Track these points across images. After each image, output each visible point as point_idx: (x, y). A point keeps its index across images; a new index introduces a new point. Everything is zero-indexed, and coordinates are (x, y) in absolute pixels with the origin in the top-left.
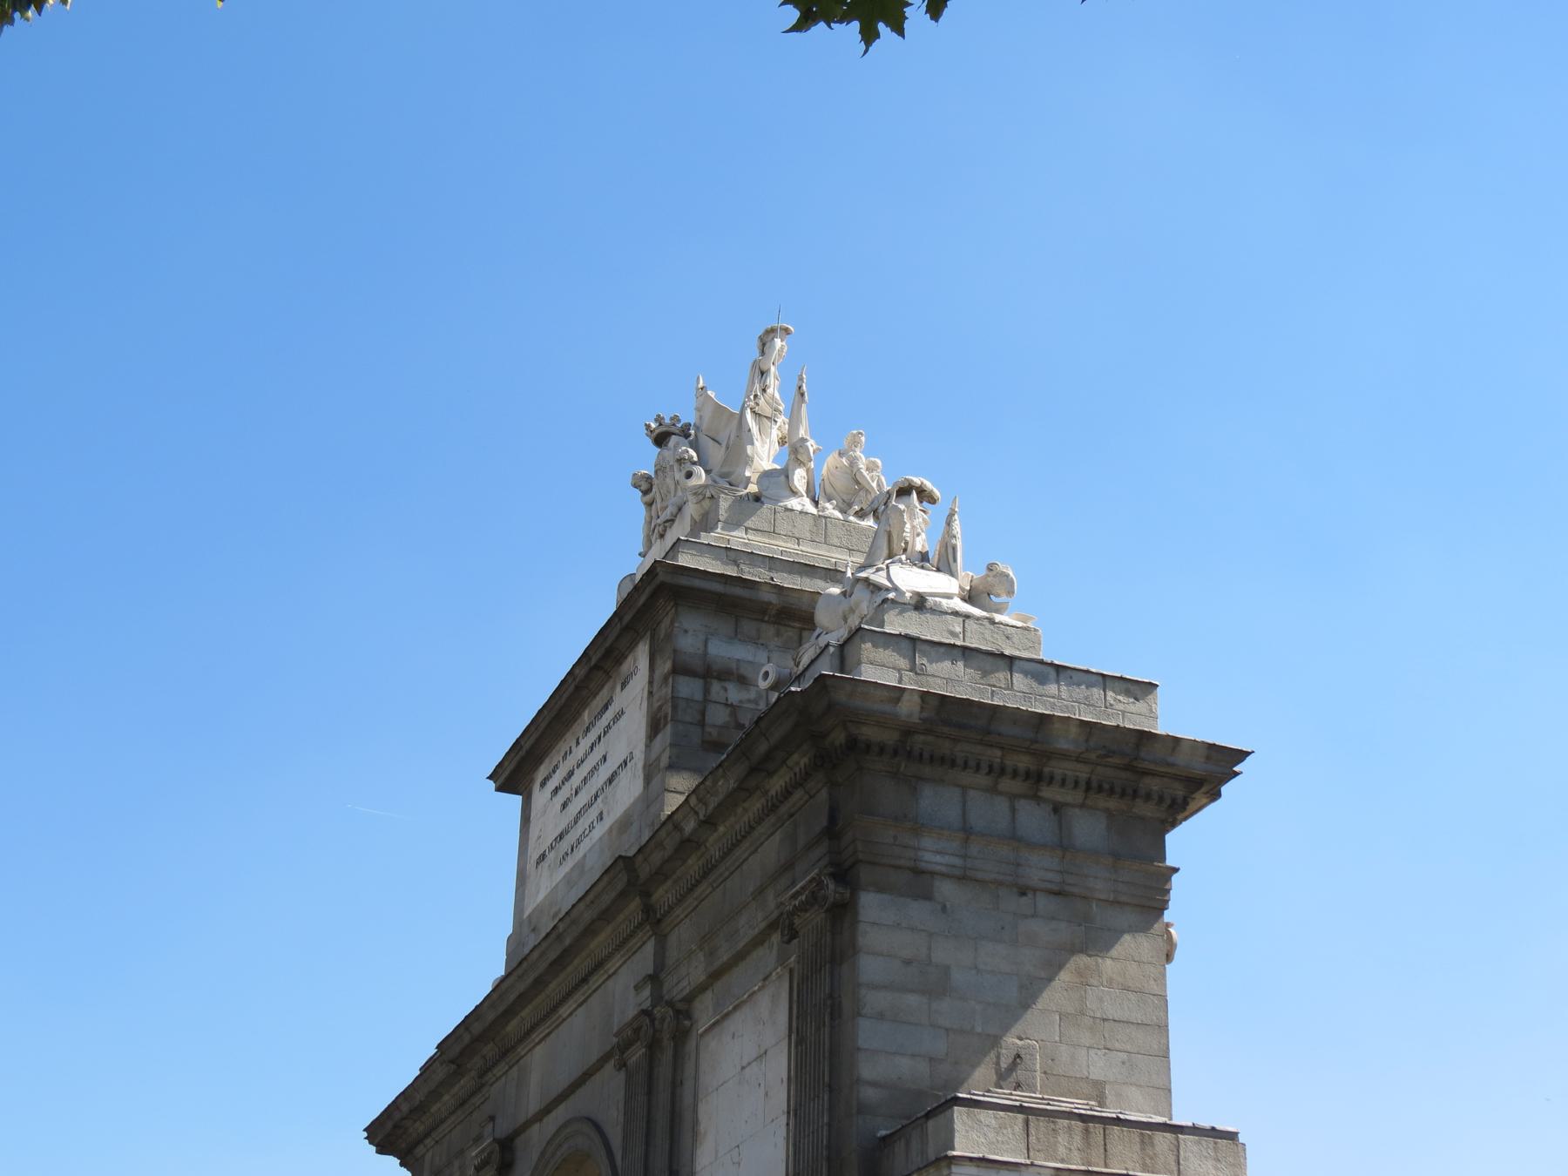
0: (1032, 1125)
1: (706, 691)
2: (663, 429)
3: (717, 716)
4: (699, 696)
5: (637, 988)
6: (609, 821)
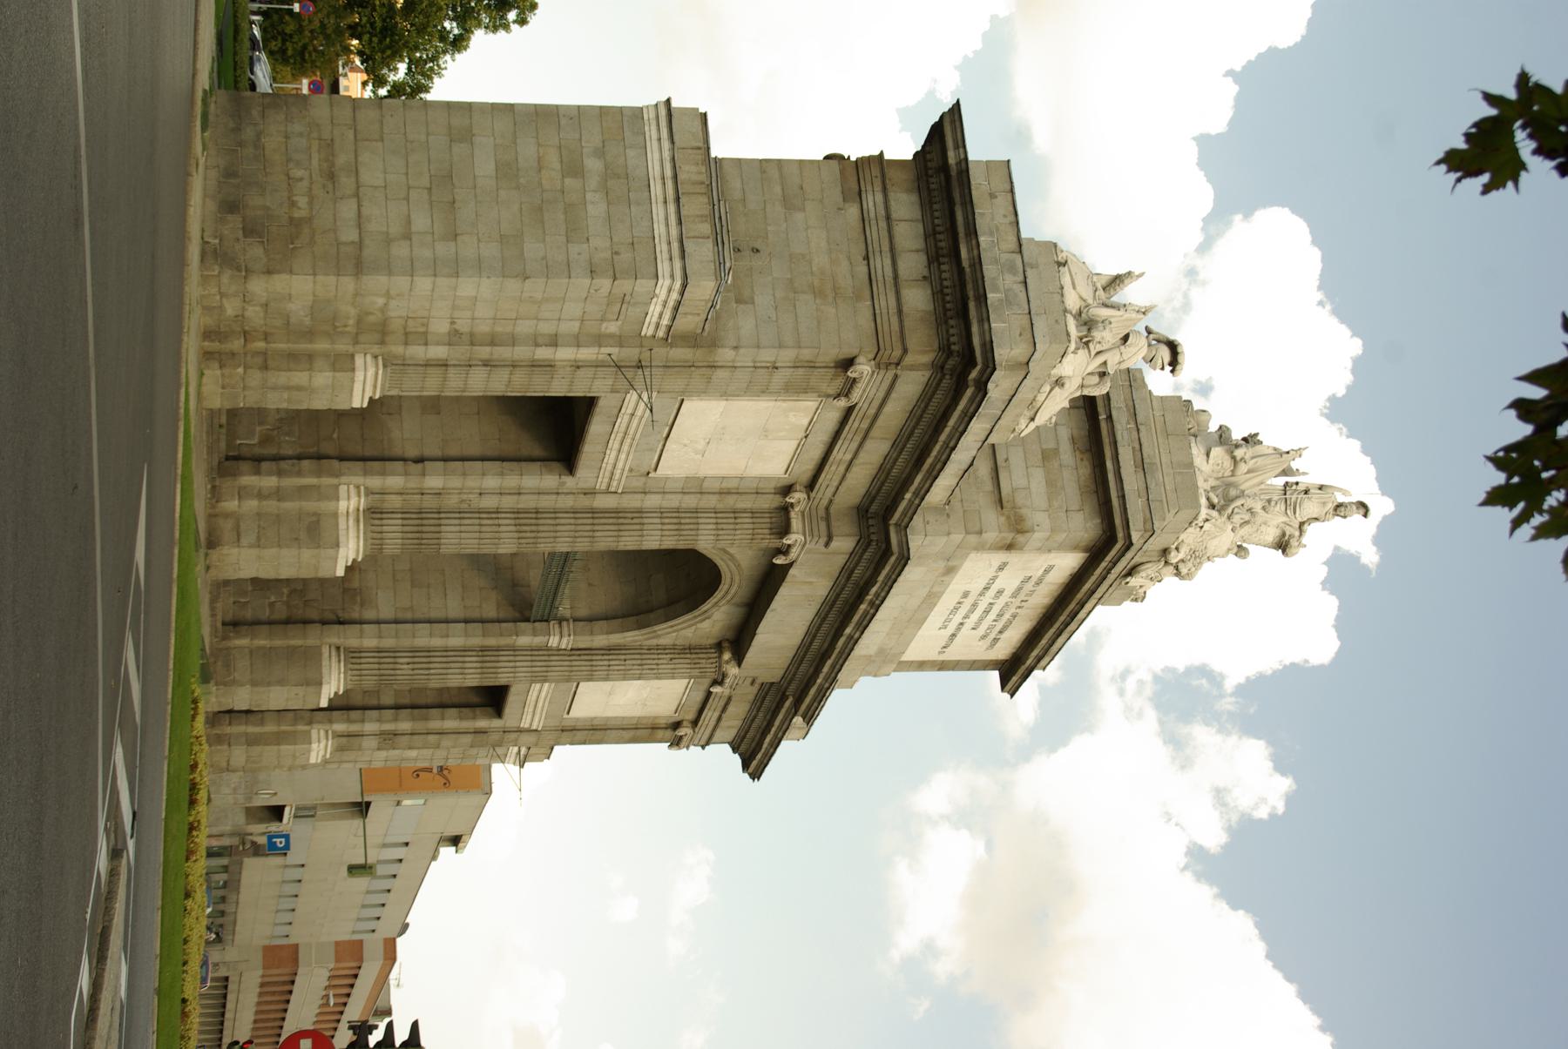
0: (699, 151)
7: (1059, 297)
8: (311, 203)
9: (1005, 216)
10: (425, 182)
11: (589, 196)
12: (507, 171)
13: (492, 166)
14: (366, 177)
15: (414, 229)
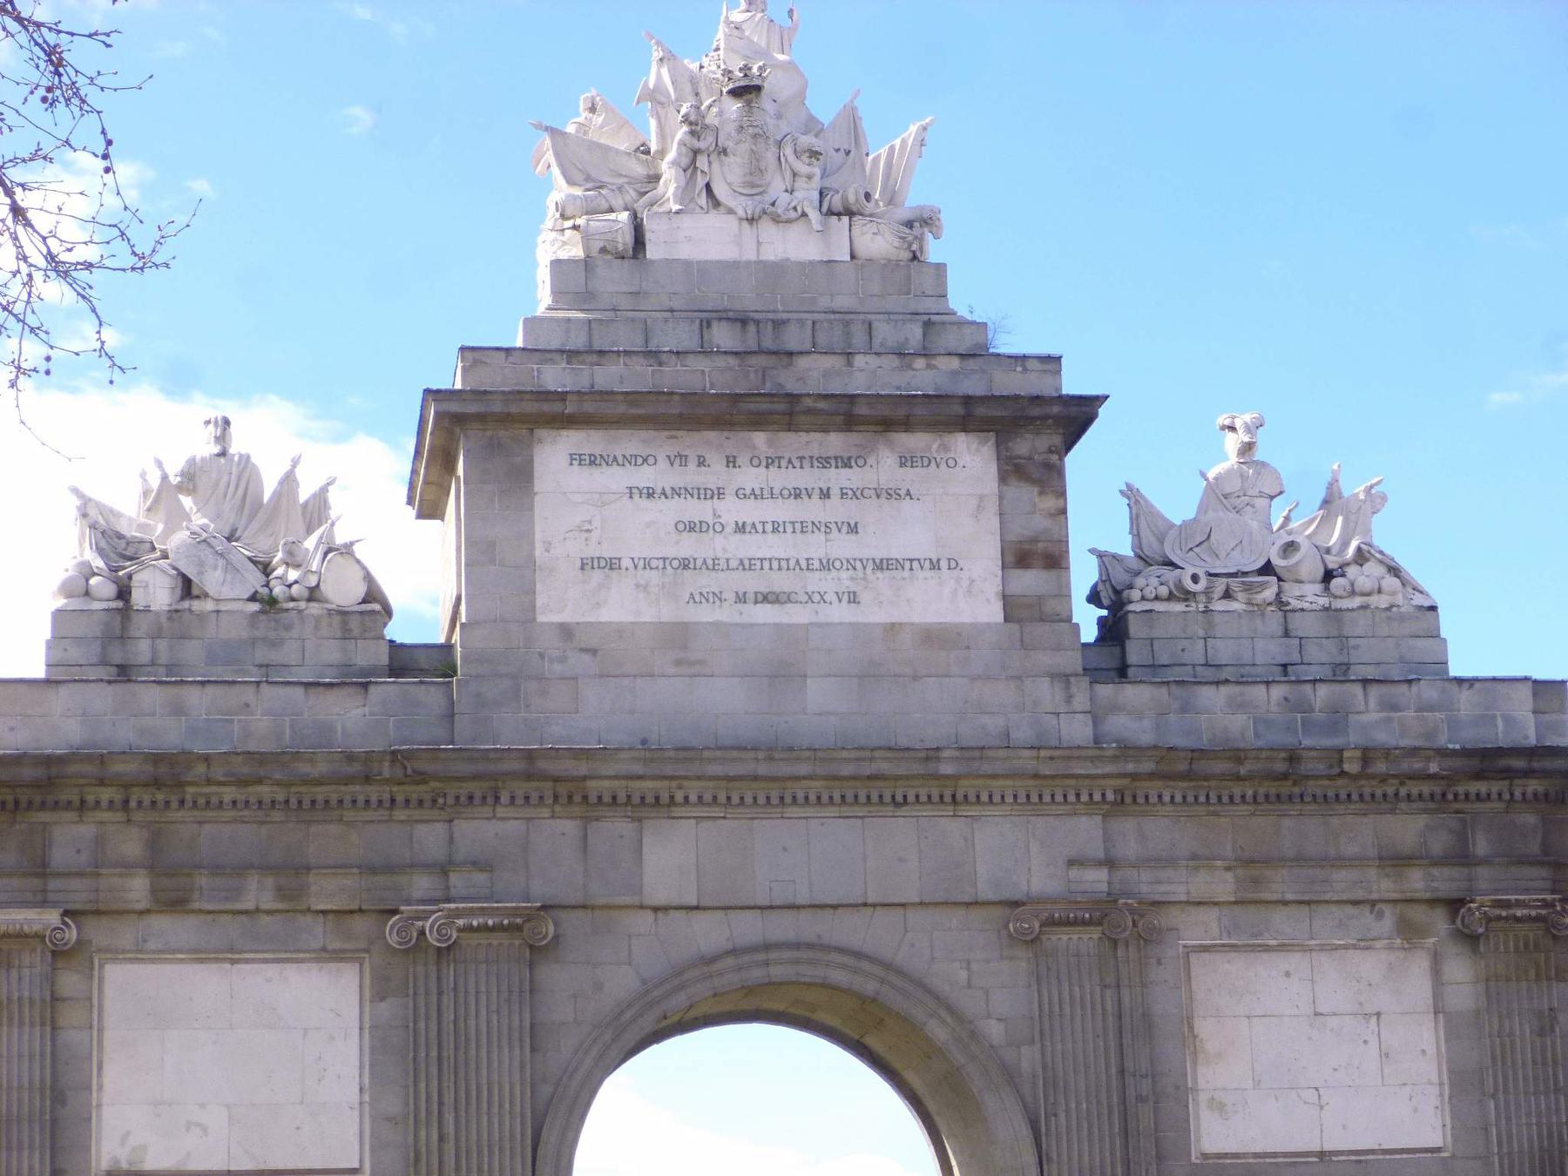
5: (1071, 863)
6: (873, 613)
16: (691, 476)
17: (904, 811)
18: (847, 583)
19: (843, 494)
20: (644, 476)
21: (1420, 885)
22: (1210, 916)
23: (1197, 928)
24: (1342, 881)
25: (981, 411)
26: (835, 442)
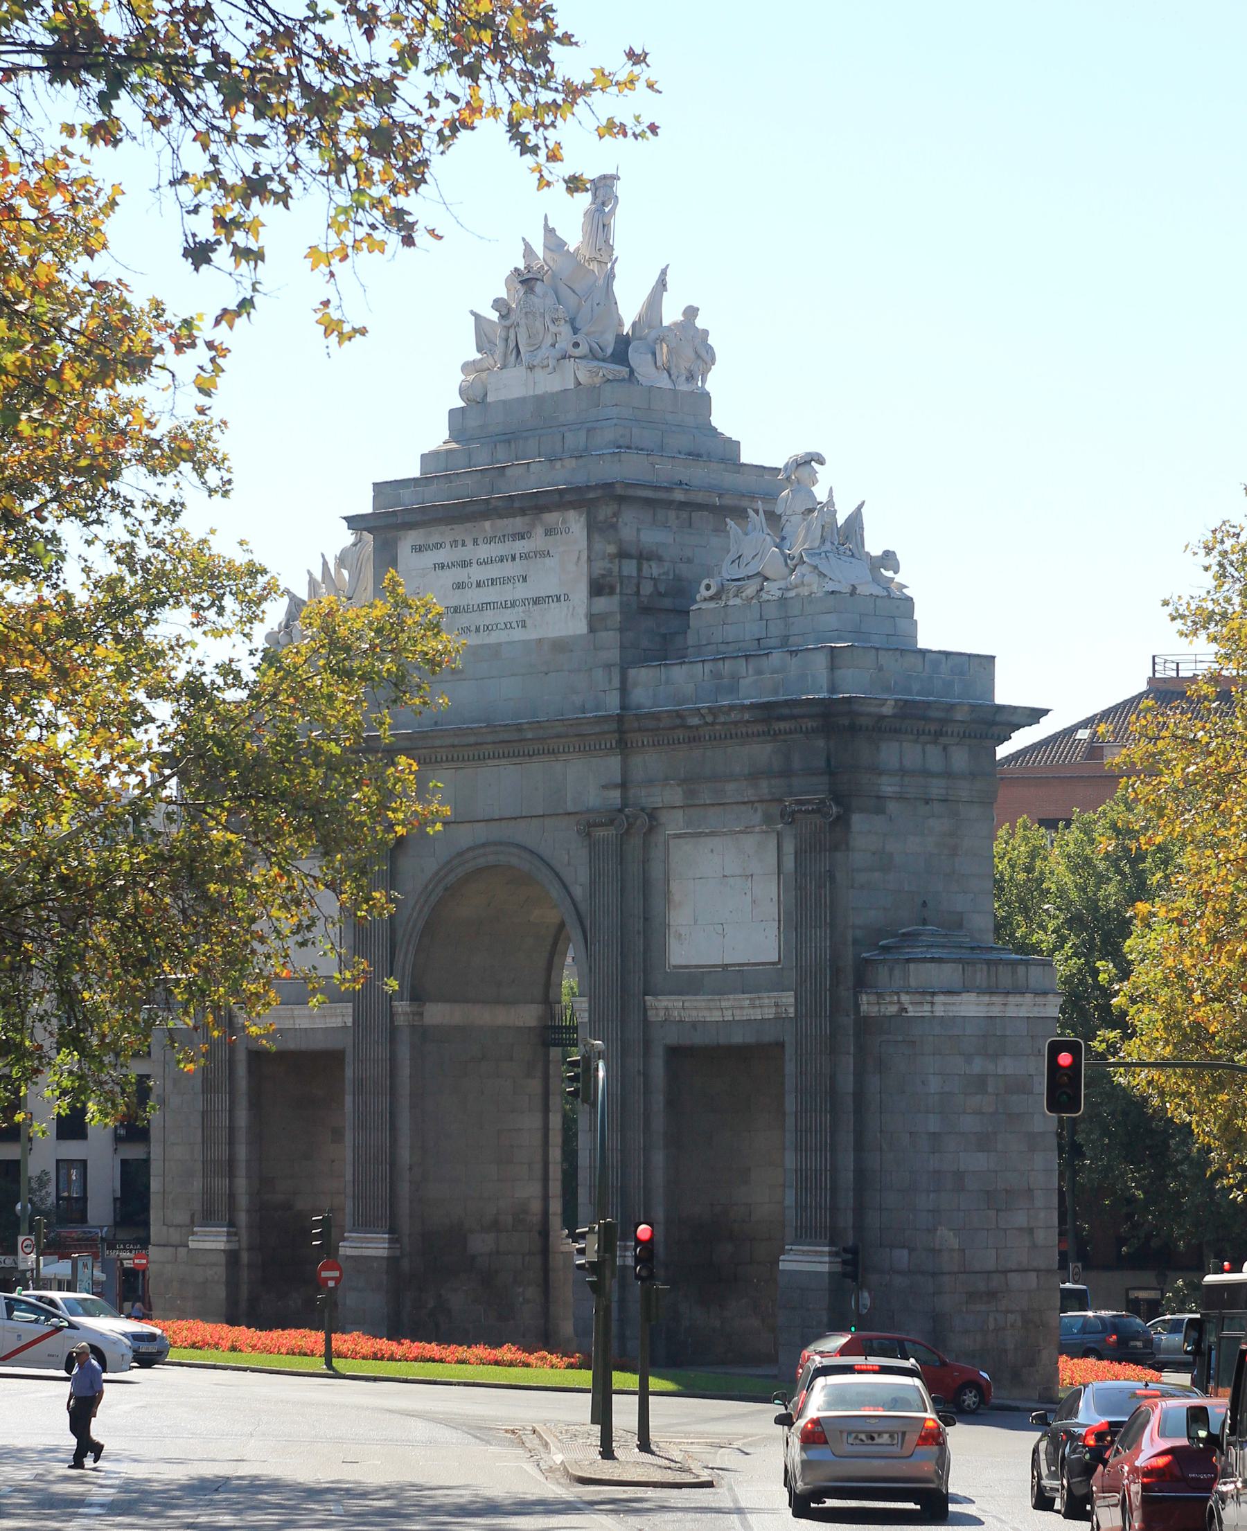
1: (640, 570)
2: (530, 276)
3: (647, 589)
4: (634, 574)
5: (605, 787)
6: (531, 634)
7: (878, 600)
8: (1012, 1312)
9: (897, 661)
10: (992, 1213)
11: (1000, 1071)
12: (984, 1142)
13: (980, 1154)
14: (991, 1265)
15: (1025, 1225)
16: (461, 553)
17: (534, 759)
18: (522, 614)
19: (521, 557)
20: (442, 556)
21: (766, 791)
22: (679, 814)
23: (673, 823)
24: (732, 790)
25: (568, 497)
26: (518, 523)
